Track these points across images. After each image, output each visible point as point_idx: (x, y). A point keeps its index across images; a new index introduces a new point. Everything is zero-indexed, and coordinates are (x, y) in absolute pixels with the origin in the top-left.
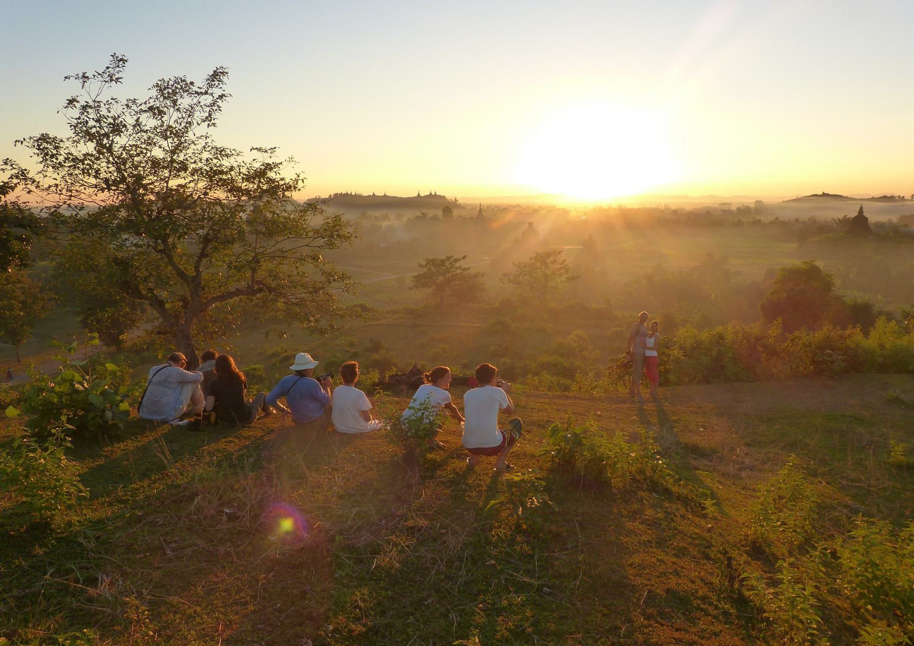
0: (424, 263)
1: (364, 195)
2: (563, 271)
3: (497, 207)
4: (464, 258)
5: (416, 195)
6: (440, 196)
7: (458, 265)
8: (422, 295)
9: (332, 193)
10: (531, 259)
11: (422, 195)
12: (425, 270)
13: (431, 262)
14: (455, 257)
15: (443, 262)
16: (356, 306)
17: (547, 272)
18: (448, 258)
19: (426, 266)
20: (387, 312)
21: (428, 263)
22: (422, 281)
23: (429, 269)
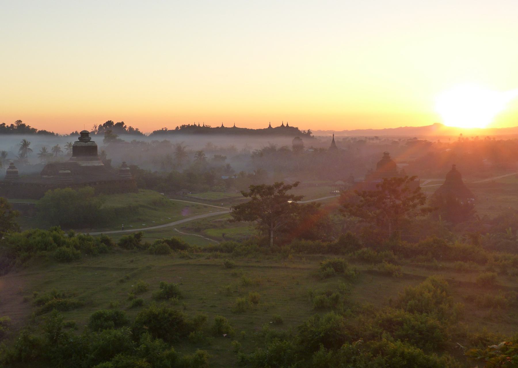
0: (249, 191)
1: (212, 127)
2: (416, 201)
3: (354, 139)
4: (296, 185)
5: (267, 127)
6: (292, 128)
7: (288, 193)
8: (249, 230)
9: (180, 125)
10: (378, 186)
11: (273, 126)
12: (249, 198)
13: (256, 189)
14: (285, 184)
15: (270, 189)
16: (167, 241)
17: (398, 202)
18: (277, 185)
19: (250, 195)
20: (205, 250)
21: (253, 191)
22: (243, 213)
23: (255, 199)
